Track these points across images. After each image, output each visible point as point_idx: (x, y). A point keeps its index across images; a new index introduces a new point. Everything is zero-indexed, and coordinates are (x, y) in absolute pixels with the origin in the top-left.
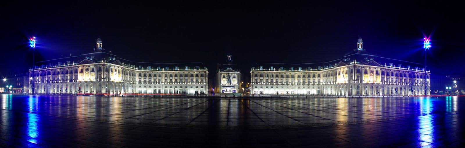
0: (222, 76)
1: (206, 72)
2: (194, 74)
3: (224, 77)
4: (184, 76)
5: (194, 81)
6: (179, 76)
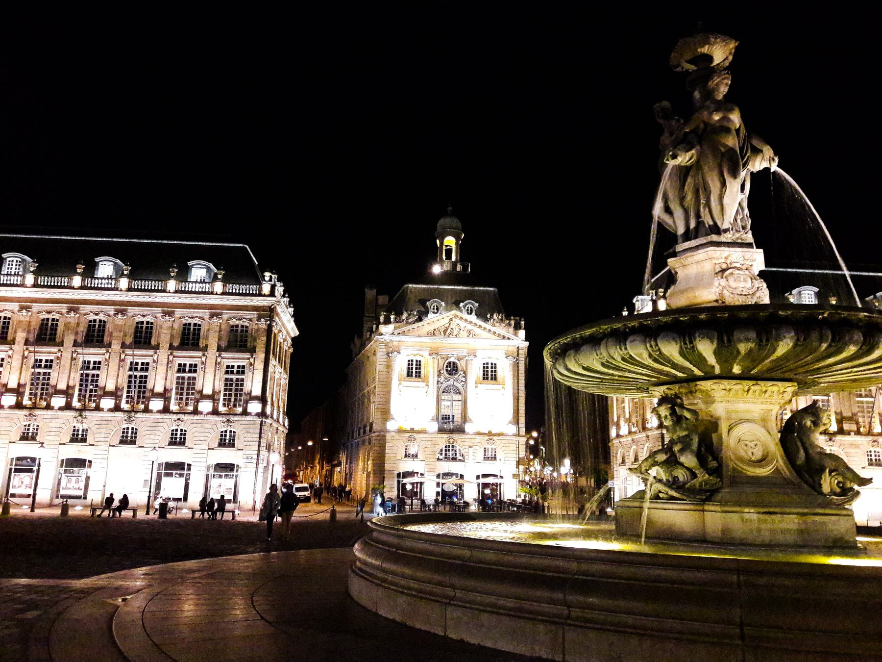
0: (400, 365)
1: (269, 313)
2: (166, 330)
3: (414, 371)
4: (69, 340)
5: (159, 389)
6: (21, 336)
